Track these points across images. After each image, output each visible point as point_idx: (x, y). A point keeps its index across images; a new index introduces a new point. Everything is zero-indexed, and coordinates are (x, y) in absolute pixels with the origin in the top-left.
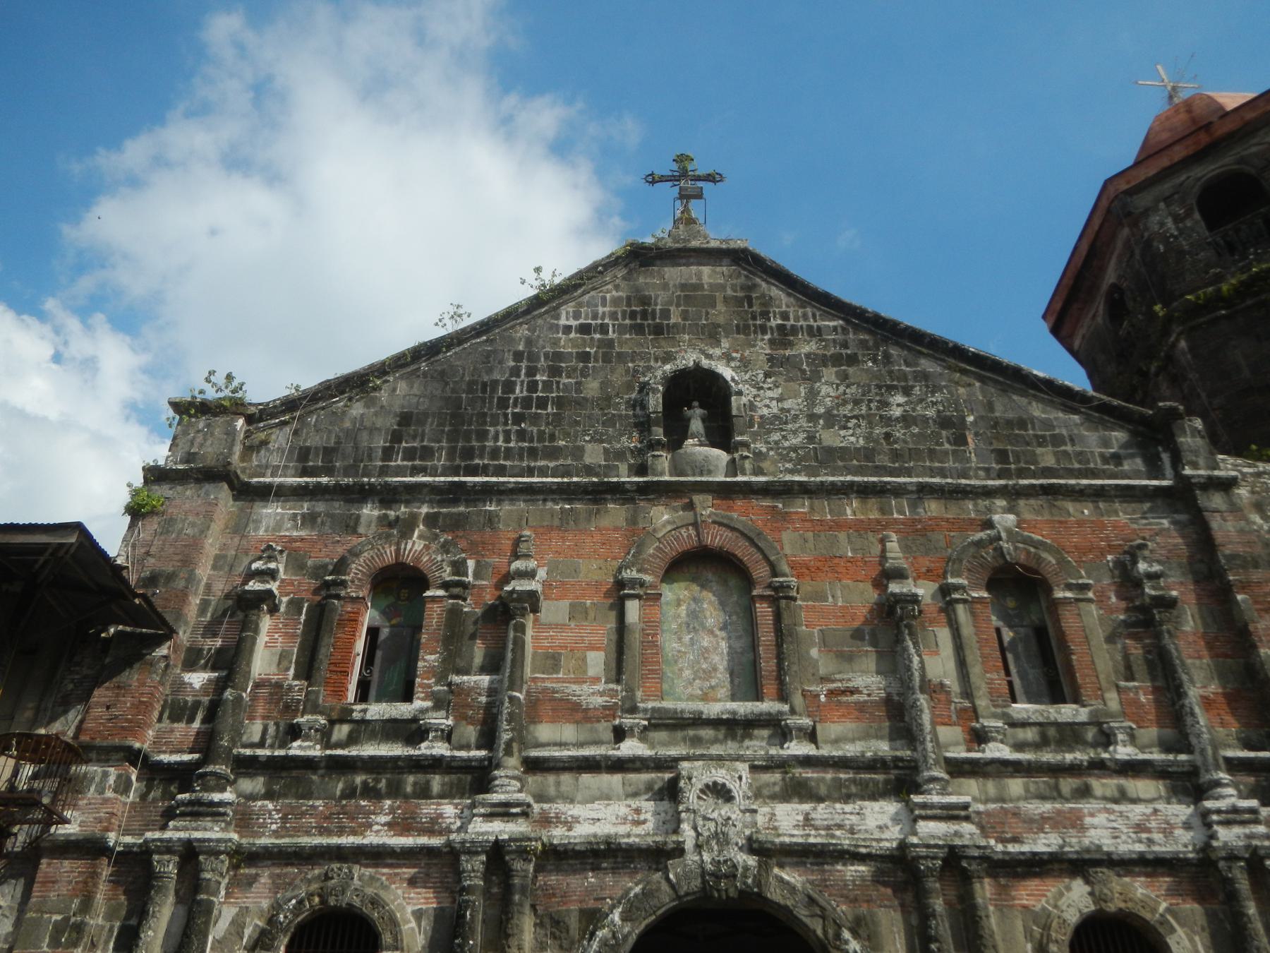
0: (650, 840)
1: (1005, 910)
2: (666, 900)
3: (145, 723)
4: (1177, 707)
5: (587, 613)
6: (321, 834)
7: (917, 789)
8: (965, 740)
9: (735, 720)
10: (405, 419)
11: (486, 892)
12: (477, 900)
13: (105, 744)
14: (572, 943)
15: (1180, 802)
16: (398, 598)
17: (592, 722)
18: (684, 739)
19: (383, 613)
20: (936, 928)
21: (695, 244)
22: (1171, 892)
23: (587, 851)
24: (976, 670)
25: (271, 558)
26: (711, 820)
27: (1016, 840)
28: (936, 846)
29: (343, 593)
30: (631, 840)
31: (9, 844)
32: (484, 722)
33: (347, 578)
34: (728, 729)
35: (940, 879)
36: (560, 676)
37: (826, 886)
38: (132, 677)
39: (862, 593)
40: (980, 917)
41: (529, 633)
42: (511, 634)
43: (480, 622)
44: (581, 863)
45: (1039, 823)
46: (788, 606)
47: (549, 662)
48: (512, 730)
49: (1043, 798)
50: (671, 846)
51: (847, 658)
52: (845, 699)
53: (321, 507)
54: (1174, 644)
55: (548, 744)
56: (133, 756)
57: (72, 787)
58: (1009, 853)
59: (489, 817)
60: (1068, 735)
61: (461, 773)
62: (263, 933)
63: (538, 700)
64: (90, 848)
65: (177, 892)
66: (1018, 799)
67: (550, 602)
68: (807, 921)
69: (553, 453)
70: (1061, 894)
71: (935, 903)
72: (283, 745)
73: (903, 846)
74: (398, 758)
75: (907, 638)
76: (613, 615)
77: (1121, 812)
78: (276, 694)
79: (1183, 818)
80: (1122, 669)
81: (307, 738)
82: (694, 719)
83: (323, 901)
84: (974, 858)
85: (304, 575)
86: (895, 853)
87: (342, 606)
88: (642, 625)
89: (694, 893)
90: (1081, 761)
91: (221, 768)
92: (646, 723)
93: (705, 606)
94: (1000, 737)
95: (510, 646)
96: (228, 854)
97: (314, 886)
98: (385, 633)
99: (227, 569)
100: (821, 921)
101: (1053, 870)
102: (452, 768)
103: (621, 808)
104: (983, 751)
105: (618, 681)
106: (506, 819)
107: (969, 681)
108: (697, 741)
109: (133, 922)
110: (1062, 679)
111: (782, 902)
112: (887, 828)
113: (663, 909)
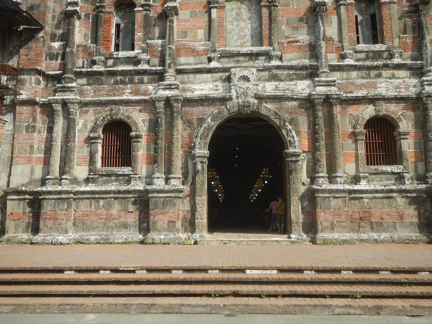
0: (220, 95)
1: (343, 115)
2: (226, 114)
3: (41, 61)
4: (421, 44)
5: (196, 15)
6: (108, 96)
7: (317, 76)
8: (337, 58)
9: (252, 53)
11: (165, 114)
12: (163, 116)
13: (28, 68)
14: (195, 128)
15: (414, 78)
16: (126, 12)
17: (200, 56)
18: (234, 61)
19: (121, 18)
20: (318, 121)
22: (404, 109)
23: (199, 99)
24: (345, 32)
26: (242, 88)
27: (351, 92)
28: (321, 95)
29: (104, 10)
30: (214, 96)
31: (5, 102)
32: (161, 57)
33: (105, 4)
34: (250, 57)
35: (322, 106)
36: (188, 39)
37: (282, 109)
38: (32, 44)
39: (304, 3)
40: (334, 118)
41: (175, 23)
42: (168, 24)
43: (157, 20)
44: (197, 104)
45: (361, 87)
46: (274, 9)
47: (183, 34)
48: (170, 59)
49: (363, 78)
50: (228, 97)
51: (296, 29)
52: (294, 44)
54: (425, 19)
55: (184, 64)
56: (39, 72)
57: (21, 83)
58: (348, 97)
59: (165, 89)
60: (377, 55)
61: (154, 75)
62: (93, 127)
63: (179, 48)
64: (31, 103)
65: (63, 116)
66: (354, 79)
67: (183, 11)
68: (274, 120)
70: (364, 110)
71: (319, 114)
72: (91, 67)
73: (310, 95)
74: (131, 70)
75: (320, 20)
76: (207, 15)
77: (391, 82)
78: (85, 49)
79: (414, 84)
80: (402, 30)
81: (99, 64)
82: (237, 54)
83: (111, 118)
84: (335, 98)
85: (88, 4)
86: (307, 98)
87: (104, 16)
88: (218, 19)
89: (236, 112)
90: (380, 64)
92: (219, 55)
93: (242, 11)
94: (351, 57)
95: (168, 28)
96: (77, 103)
97: (108, 113)
98: (122, 26)
99: (59, 3)
100: (279, 120)
101: (362, 102)
102: (151, 73)
104: (344, 62)
105: (209, 41)
106: (170, 90)
107: (342, 36)
108: (238, 61)
109: (51, 125)
110: (378, 35)
111: (266, 114)
112: (305, 89)
113: (225, 117)
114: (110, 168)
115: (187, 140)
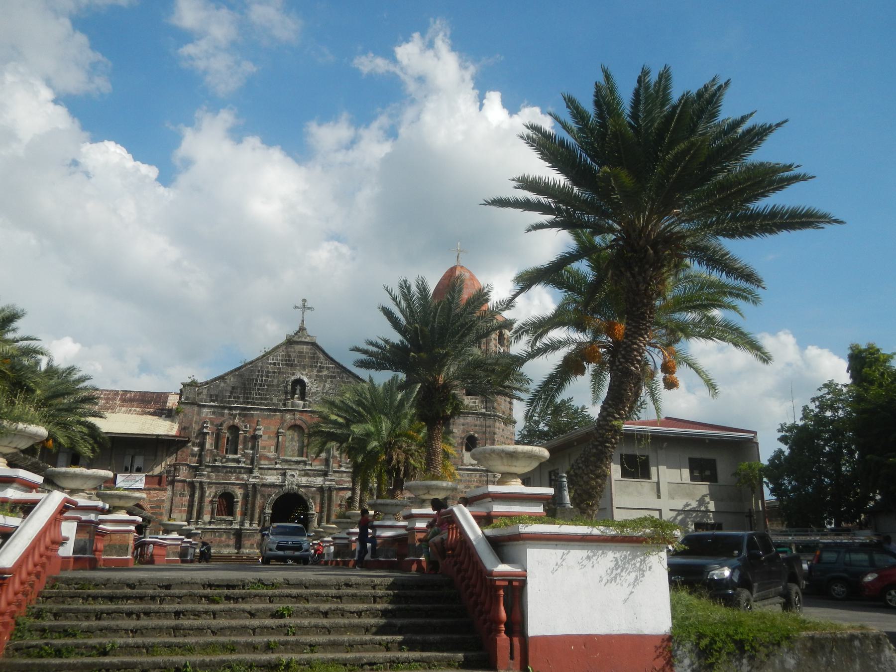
2: (282, 493)
10: (233, 388)
12: (250, 492)
21: (303, 340)
25: (207, 424)
27: (342, 485)
38: (184, 449)
53: (216, 410)
56: (187, 465)
59: (253, 478)
64: (184, 481)
69: (266, 399)
76: (276, 438)
91: (203, 467)
98: (230, 438)
103: (276, 477)
108: (290, 465)
114: (222, 517)
115: (262, 504)
